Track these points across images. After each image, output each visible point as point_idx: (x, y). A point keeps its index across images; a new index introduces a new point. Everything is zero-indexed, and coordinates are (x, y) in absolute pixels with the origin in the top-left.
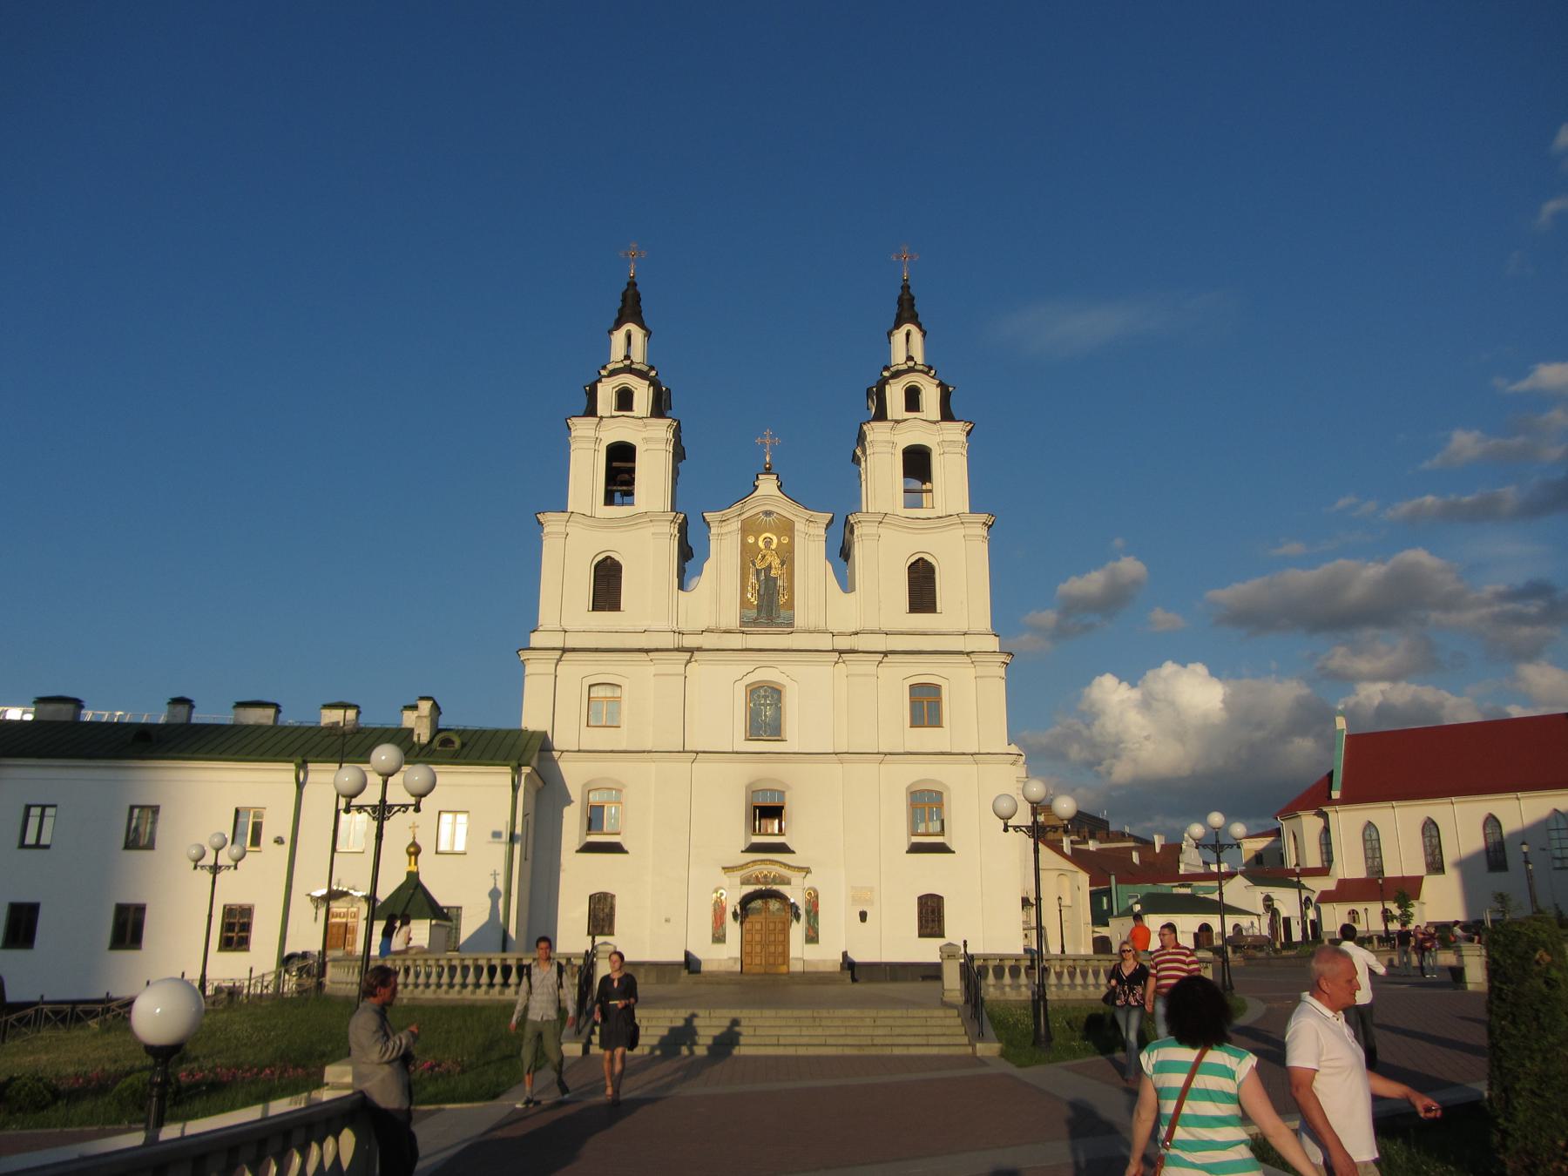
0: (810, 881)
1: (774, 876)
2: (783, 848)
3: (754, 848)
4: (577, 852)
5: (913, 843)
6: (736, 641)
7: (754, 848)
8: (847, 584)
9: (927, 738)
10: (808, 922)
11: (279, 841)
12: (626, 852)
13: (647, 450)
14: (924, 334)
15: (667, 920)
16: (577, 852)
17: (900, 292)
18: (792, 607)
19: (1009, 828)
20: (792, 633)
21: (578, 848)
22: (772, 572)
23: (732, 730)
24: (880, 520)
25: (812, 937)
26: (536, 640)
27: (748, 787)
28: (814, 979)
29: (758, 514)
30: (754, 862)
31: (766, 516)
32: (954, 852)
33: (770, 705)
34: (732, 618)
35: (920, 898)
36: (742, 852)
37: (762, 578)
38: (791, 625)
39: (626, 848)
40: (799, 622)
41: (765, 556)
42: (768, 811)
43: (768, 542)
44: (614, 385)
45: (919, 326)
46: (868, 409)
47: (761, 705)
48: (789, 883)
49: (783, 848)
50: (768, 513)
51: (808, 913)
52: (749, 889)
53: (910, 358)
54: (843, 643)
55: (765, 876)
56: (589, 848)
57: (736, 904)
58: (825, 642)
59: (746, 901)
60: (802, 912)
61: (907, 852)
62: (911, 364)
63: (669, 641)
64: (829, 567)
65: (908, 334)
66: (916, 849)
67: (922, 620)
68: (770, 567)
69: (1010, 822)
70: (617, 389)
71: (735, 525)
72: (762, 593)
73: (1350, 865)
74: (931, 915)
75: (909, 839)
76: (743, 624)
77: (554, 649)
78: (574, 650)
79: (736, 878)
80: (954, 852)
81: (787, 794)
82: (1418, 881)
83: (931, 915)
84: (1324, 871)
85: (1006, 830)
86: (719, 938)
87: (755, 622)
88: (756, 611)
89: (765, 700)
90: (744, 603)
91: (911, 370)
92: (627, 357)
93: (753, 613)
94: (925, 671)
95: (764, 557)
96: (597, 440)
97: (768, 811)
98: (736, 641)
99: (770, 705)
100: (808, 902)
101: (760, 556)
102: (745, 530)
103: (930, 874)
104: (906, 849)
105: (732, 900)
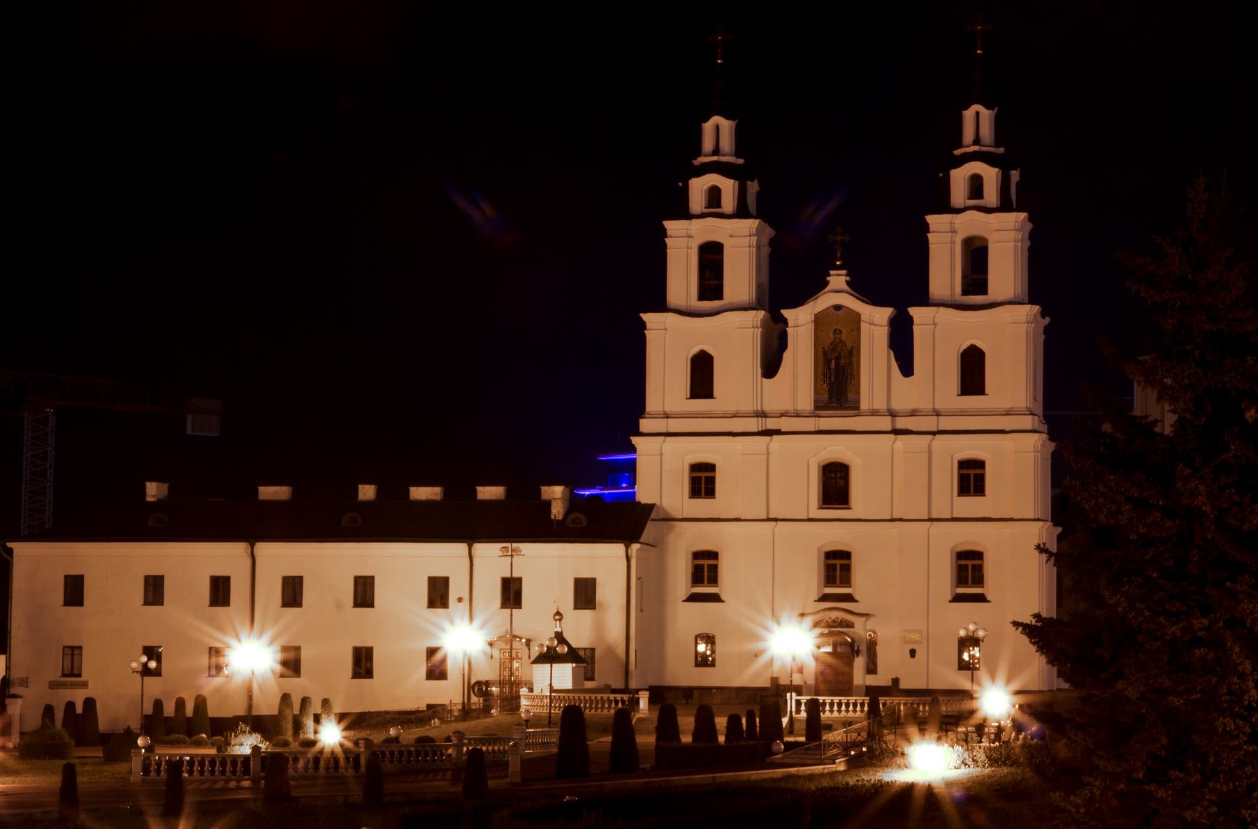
0: (870, 624)
1: (841, 621)
2: (849, 598)
3: (824, 598)
4: (684, 601)
6: (810, 424)
8: (907, 368)
9: (970, 505)
11: (460, 600)
12: (723, 601)
16: (684, 601)
18: (858, 393)
21: (685, 598)
22: (842, 361)
25: (872, 669)
26: (645, 425)
27: (819, 550)
29: (827, 309)
31: (836, 310)
32: (989, 602)
33: (840, 478)
34: (806, 402)
36: (815, 601)
37: (833, 365)
38: (858, 408)
40: (864, 405)
47: (833, 478)
48: (853, 627)
49: (849, 598)
50: (838, 307)
56: (693, 598)
58: (885, 423)
61: (950, 601)
64: (892, 353)
65: (978, 114)
66: (958, 598)
68: (838, 358)
72: (832, 380)
75: (952, 591)
76: (817, 407)
80: (989, 602)
87: (826, 407)
88: (827, 396)
89: (836, 474)
90: (816, 392)
93: (826, 397)
95: (833, 348)
98: (810, 424)
99: (840, 478)
104: (950, 598)
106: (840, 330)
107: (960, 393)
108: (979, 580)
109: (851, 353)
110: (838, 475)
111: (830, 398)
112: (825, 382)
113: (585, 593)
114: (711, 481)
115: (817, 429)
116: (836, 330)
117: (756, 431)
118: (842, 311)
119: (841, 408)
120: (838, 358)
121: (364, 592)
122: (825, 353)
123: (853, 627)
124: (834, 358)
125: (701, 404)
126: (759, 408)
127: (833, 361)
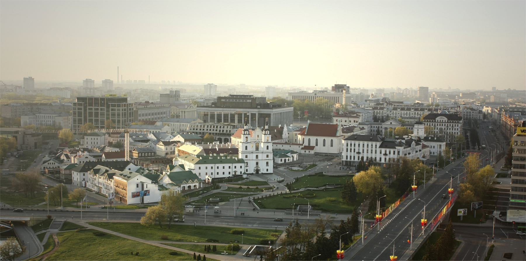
7: (256, 166)
9: (268, 158)
23: (255, 158)
25: (260, 172)
28: (260, 174)
34: (255, 151)
42: (257, 163)
54: (262, 152)
66: (267, 166)
67: (268, 150)
73: (306, 143)
74: (267, 170)
82: (315, 146)
83: (267, 170)
84: (302, 145)
86: (254, 172)
94: (267, 154)
97: (257, 163)
103: (267, 167)
105: (255, 170)
108: (268, 164)
113: (241, 167)
114: (247, 157)
121: (224, 167)
125: (246, 150)
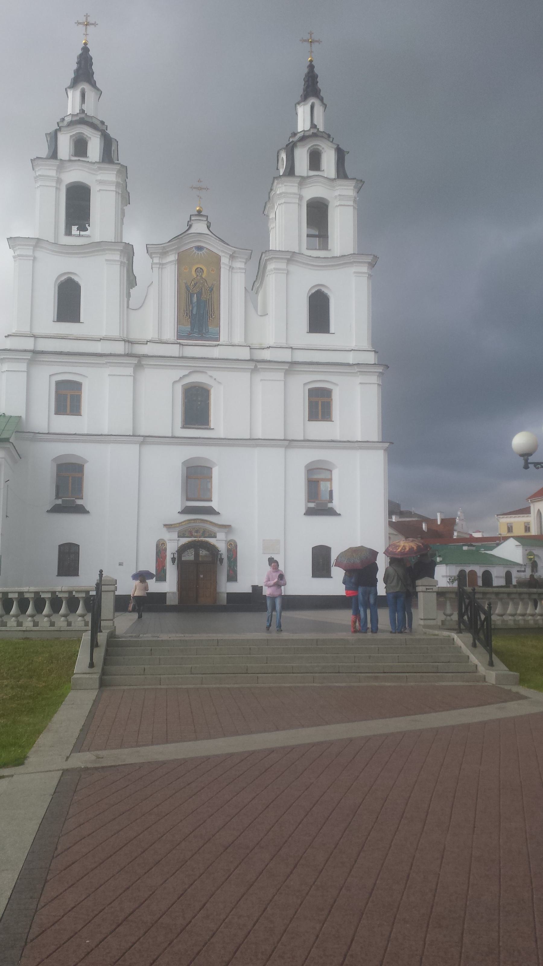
2: (211, 511)
3: (186, 511)
5: (309, 508)
10: (229, 566)
13: (100, 190)
14: (325, 106)
15: (121, 564)
16: (48, 511)
17: (306, 70)
19: (530, 465)
20: (218, 345)
24: (289, 257)
25: (232, 577)
30: (189, 521)
32: (340, 515)
35: (313, 549)
37: (195, 299)
38: (218, 339)
39: (88, 508)
40: (223, 338)
41: (197, 283)
43: (199, 271)
44: (71, 134)
45: (322, 100)
46: (277, 169)
48: (216, 537)
50: (200, 248)
51: (229, 558)
52: (184, 541)
53: (313, 126)
55: (197, 531)
57: (174, 552)
59: (182, 550)
60: (225, 556)
62: (315, 131)
63: (119, 348)
67: (319, 339)
68: (199, 294)
69: (531, 459)
70: (74, 138)
71: (172, 257)
72: (194, 312)
75: (306, 505)
76: (179, 337)
77: (25, 351)
78: (43, 353)
79: (175, 535)
81: (213, 469)
85: (526, 467)
87: (189, 337)
90: (179, 322)
91: (315, 135)
92: (83, 111)
93: (188, 328)
95: (195, 284)
96: (59, 181)
98: (174, 350)
100: (229, 550)
101: (193, 282)
102: (180, 262)
104: (304, 511)
105: (171, 548)
106: (201, 268)
107: (308, 331)
109: (211, 290)
110: (199, 399)
111: (192, 329)
112: (187, 313)
115: (181, 355)
116: (198, 268)
117: (123, 353)
118: (203, 251)
119: (202, 338)
120: (199, 294)
122: (187, 288)
123: (216, 537)
124: (196, 293)
126: (125, 336)
127: (195, 295)
